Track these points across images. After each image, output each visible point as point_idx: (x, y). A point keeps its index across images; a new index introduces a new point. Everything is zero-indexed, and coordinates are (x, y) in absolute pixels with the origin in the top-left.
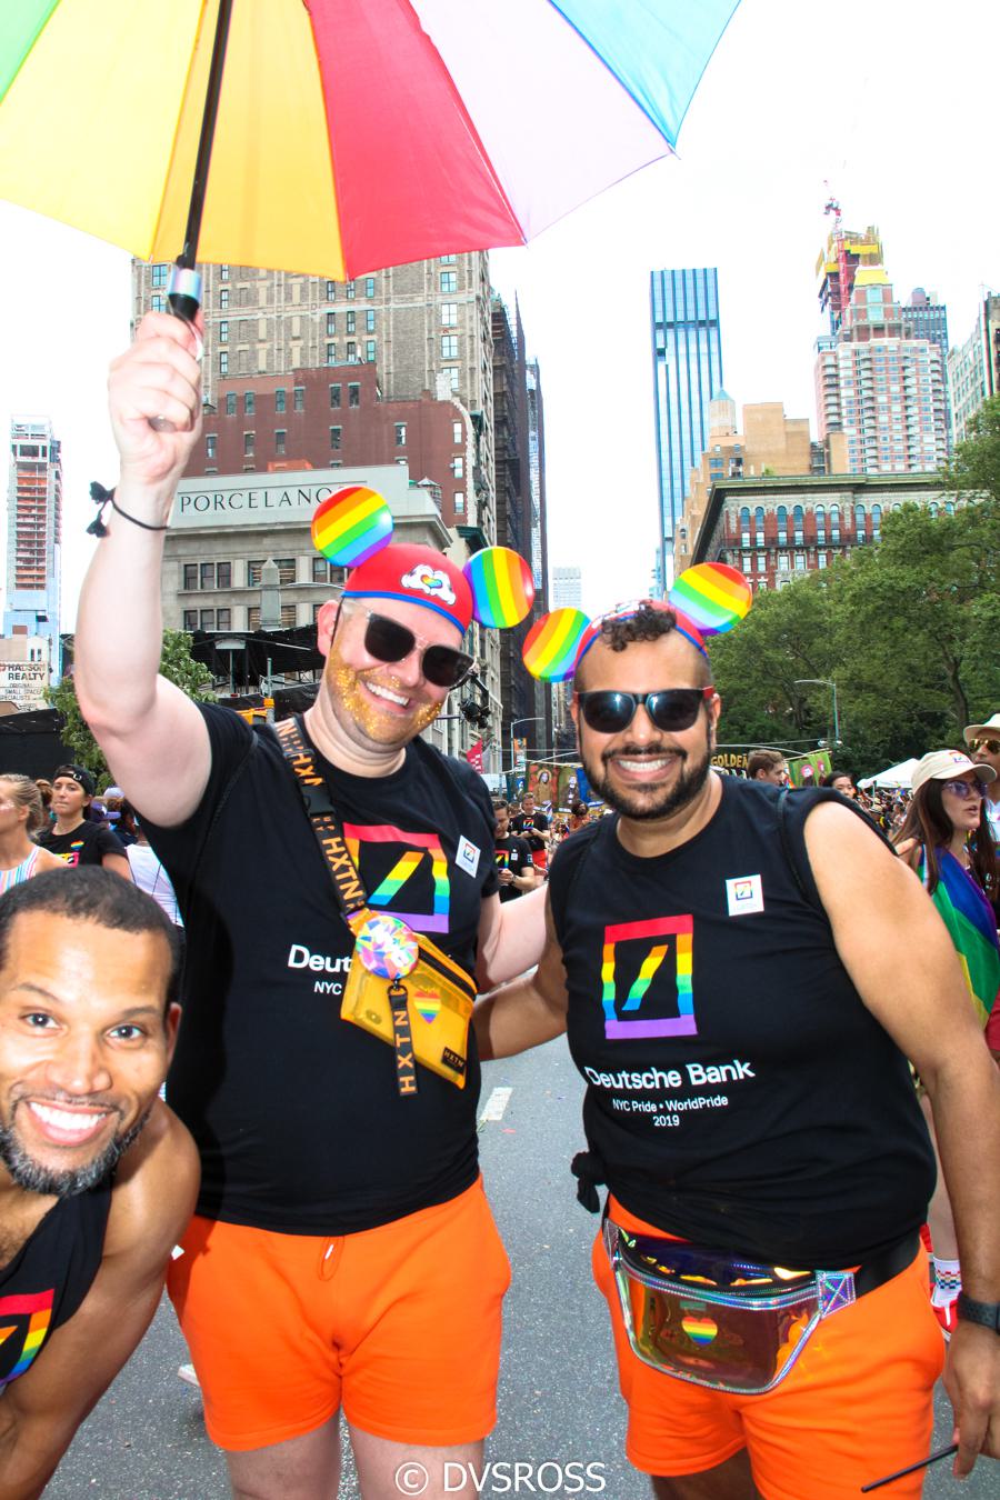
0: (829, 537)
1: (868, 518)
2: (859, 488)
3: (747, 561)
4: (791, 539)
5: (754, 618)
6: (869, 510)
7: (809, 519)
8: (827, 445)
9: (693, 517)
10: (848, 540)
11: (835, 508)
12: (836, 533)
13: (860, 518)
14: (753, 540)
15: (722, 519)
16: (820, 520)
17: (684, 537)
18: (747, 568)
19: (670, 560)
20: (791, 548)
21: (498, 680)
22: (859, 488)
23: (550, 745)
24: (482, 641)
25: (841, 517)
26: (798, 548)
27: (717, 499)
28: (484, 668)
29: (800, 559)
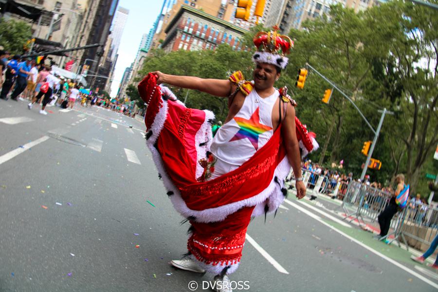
0: (212, 39)
1: (227, 38)
2: (228, 28)
3: (184, 36)
4: (200, 35)
5: (176, 57)
6: (228, 36)
7: (209, 30)
8: (226, 6)
9: (174, 12)
10: (218, 42)
11: (218, 31)
12: (215, 39)
13: (224, 39)
14: (188, 30)
15: (181, 19)
16: (212, 32)
17: (168, 17)
18: (183, 39)
19: (161, 23)
20: (199, 38)
21: (86, 42)
22: (228, 28)
23: (96, 71)
24: (85, 26)
25: (219, 34)
26: (202, 39)
27: (183, 11)
28: (82, 36)
29: (201, 43)
